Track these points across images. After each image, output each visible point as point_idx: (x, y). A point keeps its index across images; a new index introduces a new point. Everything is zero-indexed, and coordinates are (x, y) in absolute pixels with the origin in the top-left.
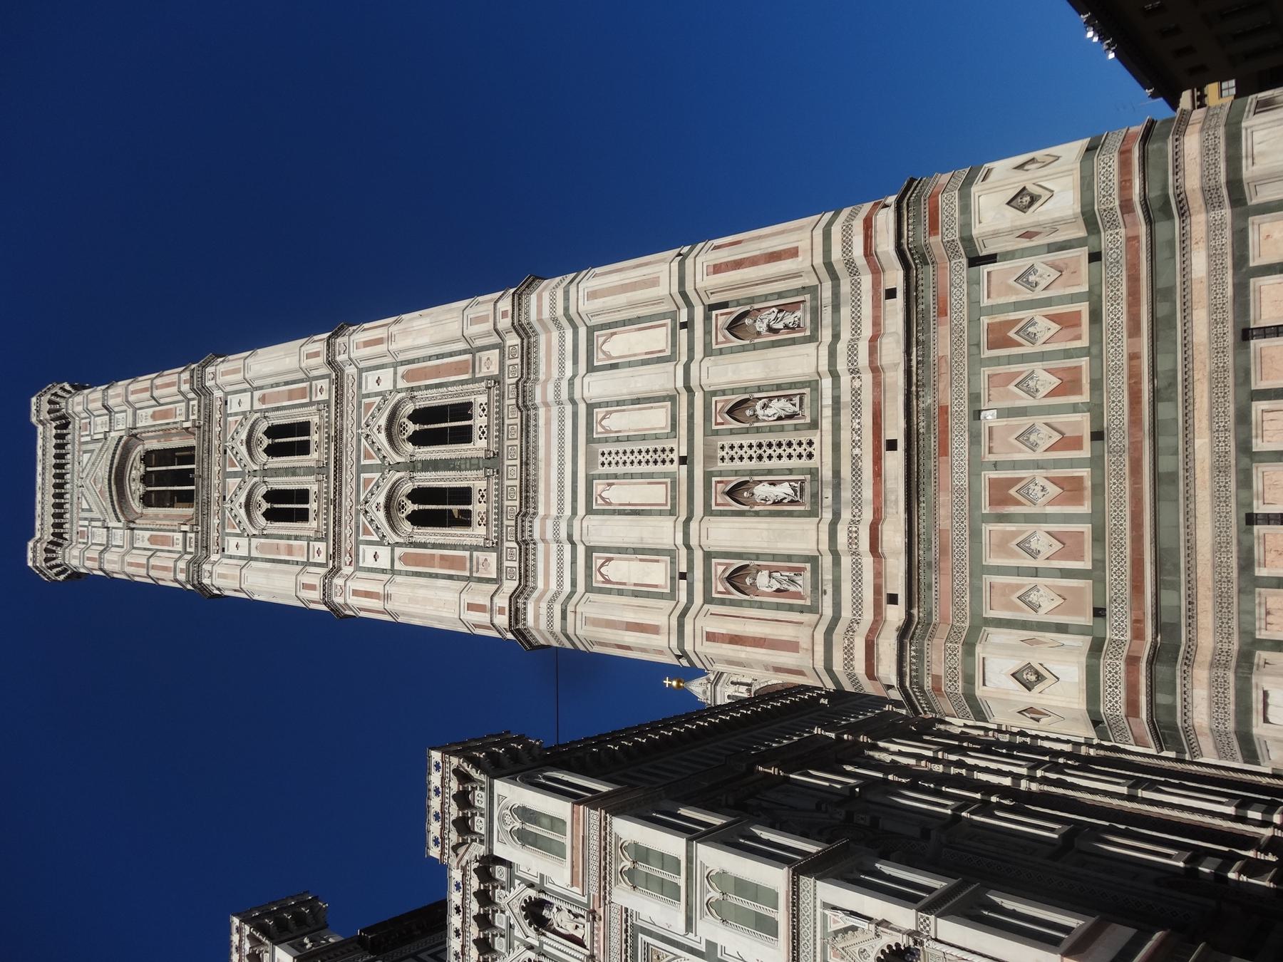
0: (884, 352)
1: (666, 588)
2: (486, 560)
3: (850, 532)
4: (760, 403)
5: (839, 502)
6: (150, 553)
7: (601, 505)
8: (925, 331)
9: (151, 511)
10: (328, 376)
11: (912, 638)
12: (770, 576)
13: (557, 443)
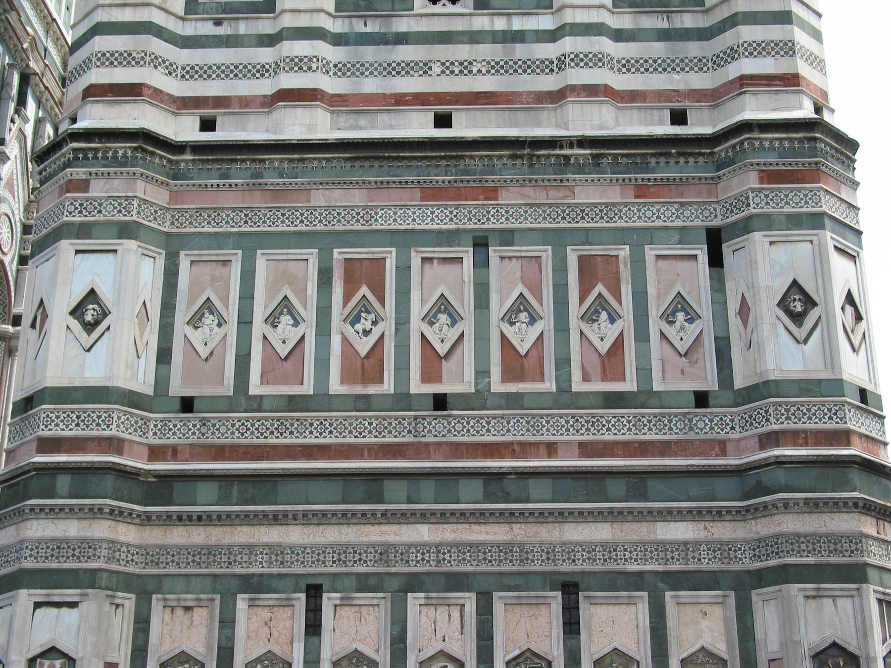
0: (587, 107)
3: (310, 60)
5: (357, 44)
8: (616, 167)
11: (144, 150)
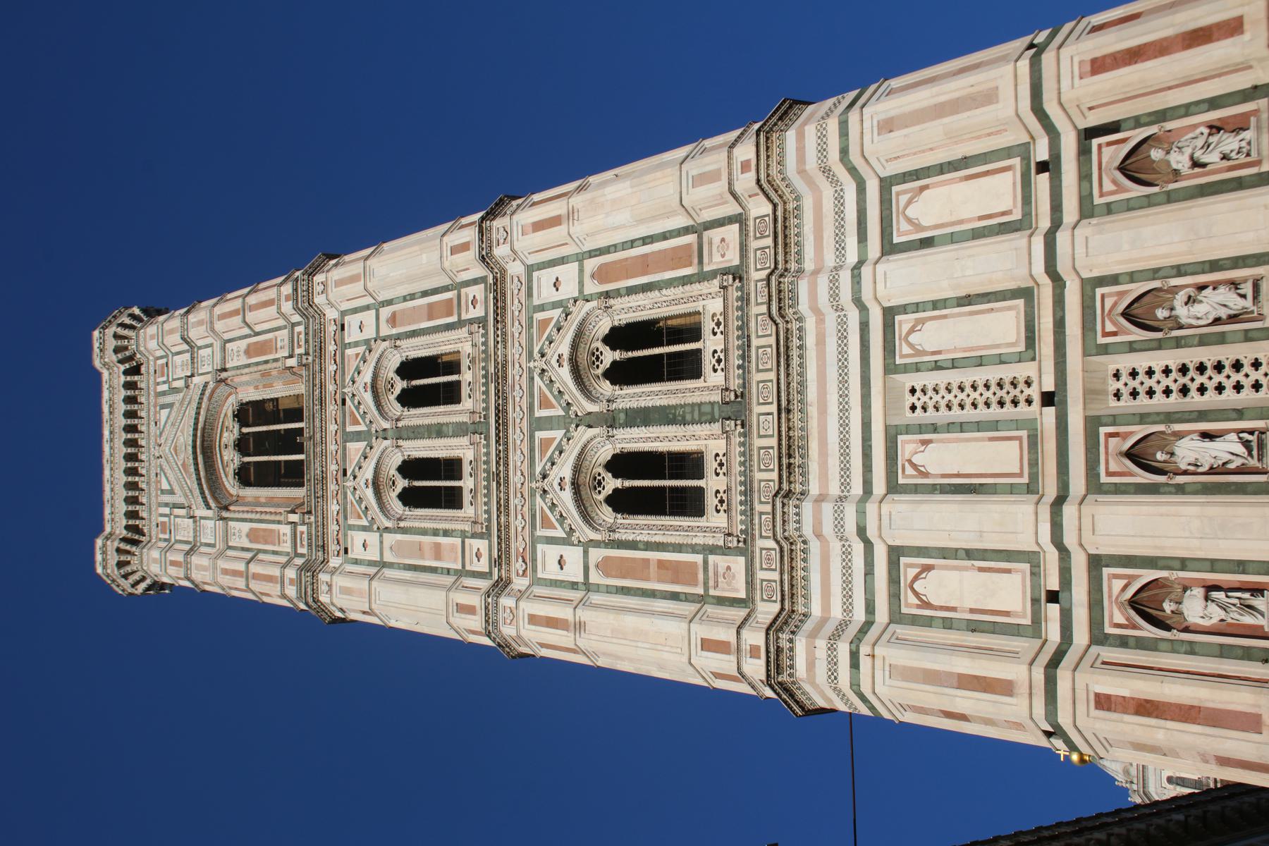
1: (1024, 617)
2: (729, 568)
4: (1181, 297)
6: (248, 555)
7: (912, 476)
9: (251, 493)
10: (483, 280)
12: (1207, 598)
13: (836, 375)
